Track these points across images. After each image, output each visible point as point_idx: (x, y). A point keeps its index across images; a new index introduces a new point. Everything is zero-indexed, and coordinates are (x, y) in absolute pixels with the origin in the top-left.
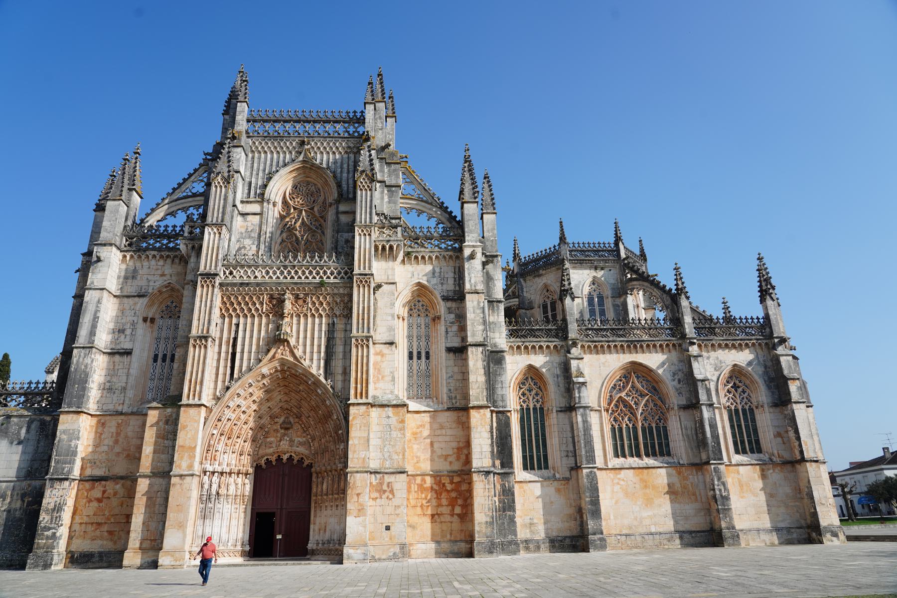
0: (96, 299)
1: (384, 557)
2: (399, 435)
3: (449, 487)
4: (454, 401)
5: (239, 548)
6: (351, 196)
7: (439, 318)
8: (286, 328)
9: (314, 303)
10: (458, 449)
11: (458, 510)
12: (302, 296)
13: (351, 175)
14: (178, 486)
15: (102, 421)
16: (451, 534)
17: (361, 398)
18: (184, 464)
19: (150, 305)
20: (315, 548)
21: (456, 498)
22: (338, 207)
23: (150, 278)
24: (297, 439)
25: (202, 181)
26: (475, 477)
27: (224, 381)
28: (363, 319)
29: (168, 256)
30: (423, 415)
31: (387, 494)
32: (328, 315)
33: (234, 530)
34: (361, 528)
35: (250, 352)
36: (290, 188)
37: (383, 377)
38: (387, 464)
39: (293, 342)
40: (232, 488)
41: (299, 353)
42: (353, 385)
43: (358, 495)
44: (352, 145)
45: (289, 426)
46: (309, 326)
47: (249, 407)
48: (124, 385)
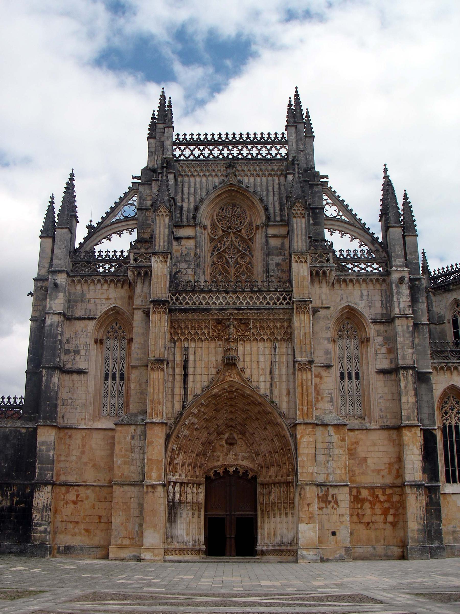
0: (56, 324)
1: (330, 558)
2: (341, 452)
3: (382, 498)
4: (385, 420)
6: (278, 219)
7: (368, 340)
10: (389, 464)
11: (390, 519)
13: (277, 197)
15: (69, 434)
16: (384, 540)
18: (154, 475)
19: (99, 327)
20: (265, 548)
21: (389, 508)
22: (266, 231)
23: (98, 301)
25: (132, 204)
26: (408, 490)
29: (112, 281)
30: (357, 432)
31: (332, 504)
34: (312, 533)
36: (217, 210)
37: (322, 398)
38: (331, 478)
39: (240, 365)
44: (276, 168)
45: (234, 441)
48: (84, 401)
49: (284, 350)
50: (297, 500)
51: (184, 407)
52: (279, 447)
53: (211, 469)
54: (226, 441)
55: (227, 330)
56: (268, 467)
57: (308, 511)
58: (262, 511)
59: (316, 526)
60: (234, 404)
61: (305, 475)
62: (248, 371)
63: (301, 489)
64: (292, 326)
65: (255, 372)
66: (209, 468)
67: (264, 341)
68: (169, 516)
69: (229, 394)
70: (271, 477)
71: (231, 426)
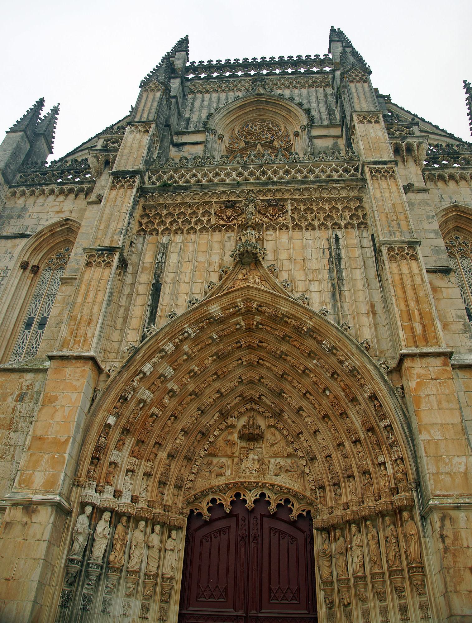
14: (17, 529)
18: (39, 479)
45: (257, 431)
49: (355, 242)
50: (432, 562)
51: (144, 337)
52: (363, 424)
53: (204, 494)
54: (240, 432)
56: (337, 485)
58: (330, 605)
61: (448, 479)
62: (284, 276)
65: (299, 276)
66: (198, 491)
67: (314, 229)
68: (64, 605)
71: (252, 400)
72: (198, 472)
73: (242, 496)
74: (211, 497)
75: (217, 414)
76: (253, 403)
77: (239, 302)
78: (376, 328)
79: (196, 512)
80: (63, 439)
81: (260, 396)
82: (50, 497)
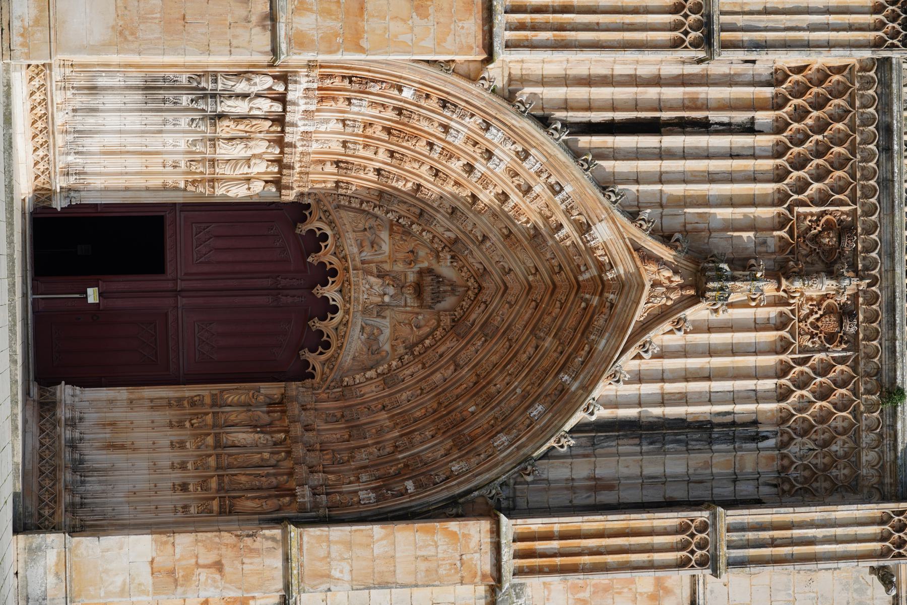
5: (60, 182)
8: (740, 291)
9: (824, 369)
12: (850, 329)
14: (241, 12)
17: (518, 555)
18: (306, 23)
20: (63, 413)
24: (386, 325)
27: (566, 106)
28: (773, 543)
32: (784, 418)
33: (114, 164)
34: (119, 581)
35: (661, 178)
40: (238, 151)
41: (660, 336)
42: (558, 524)
43: (218, 566)
46: (749, 361)
47: (485, 181)
54: (430, 271)
55: (820, 266)
57: (198, 565)
59: (145, 592)
60: (560, 295)
61: (322, 553)
63: (273, 539)
64: (836, 497)
66: (335, 215)
69: (593, 278)
70: (307, 428)
72: (364, 211)
73: (333, 279)
74: (329, 232)
75: (453, 236)
76: (476, 291)
77: (618, 270)
78: (567, 488)
79: (307, 213)
80: (364, 44)
81: (485, 302)
82: (283, 47)
